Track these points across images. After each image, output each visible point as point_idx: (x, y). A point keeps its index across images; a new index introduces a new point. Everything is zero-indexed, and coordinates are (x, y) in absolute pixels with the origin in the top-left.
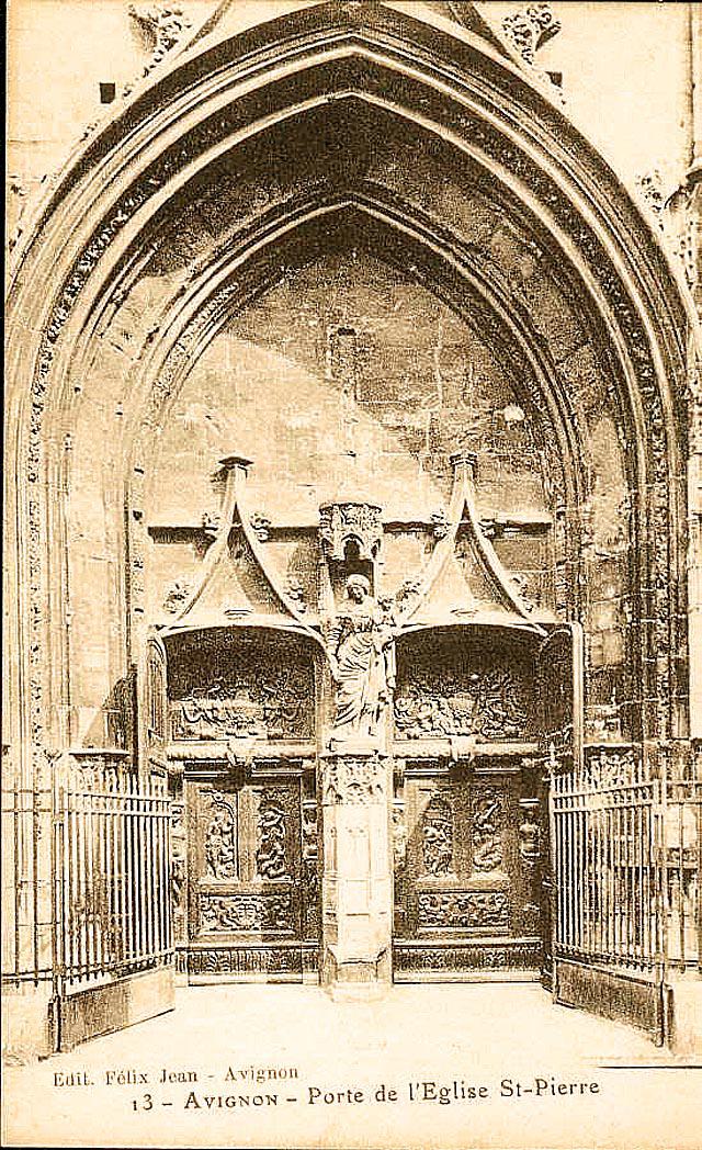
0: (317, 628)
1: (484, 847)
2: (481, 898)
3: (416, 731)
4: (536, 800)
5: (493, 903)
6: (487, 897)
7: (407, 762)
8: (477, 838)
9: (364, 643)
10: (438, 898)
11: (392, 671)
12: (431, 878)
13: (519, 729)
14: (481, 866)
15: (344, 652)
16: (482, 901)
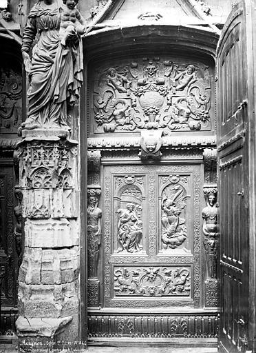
0: (17, 32)
1: (171, 226)
2: (167, 271)
3: (112, 125)
4: (216, 185)
5: (178, 276)
6: (173, 270)
7: (101, 151)
8: (165, 219)
9: (54, 40)
10: (130, 270)
11: (81, 66)
12: (125, 253)
13: (202, 123)
14: (168, 243)
15: (36, 49)
16: (168, 274)
